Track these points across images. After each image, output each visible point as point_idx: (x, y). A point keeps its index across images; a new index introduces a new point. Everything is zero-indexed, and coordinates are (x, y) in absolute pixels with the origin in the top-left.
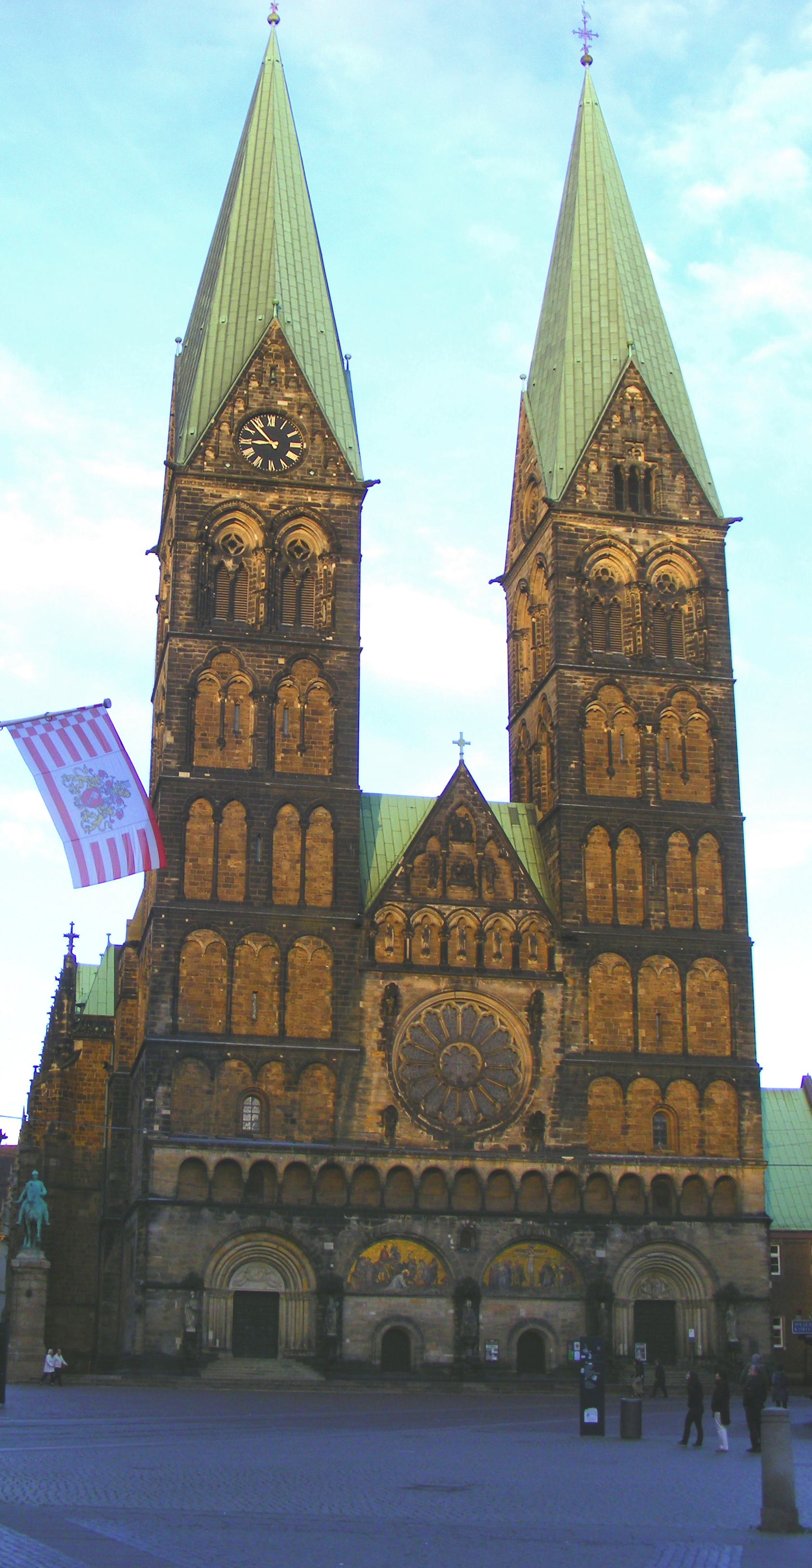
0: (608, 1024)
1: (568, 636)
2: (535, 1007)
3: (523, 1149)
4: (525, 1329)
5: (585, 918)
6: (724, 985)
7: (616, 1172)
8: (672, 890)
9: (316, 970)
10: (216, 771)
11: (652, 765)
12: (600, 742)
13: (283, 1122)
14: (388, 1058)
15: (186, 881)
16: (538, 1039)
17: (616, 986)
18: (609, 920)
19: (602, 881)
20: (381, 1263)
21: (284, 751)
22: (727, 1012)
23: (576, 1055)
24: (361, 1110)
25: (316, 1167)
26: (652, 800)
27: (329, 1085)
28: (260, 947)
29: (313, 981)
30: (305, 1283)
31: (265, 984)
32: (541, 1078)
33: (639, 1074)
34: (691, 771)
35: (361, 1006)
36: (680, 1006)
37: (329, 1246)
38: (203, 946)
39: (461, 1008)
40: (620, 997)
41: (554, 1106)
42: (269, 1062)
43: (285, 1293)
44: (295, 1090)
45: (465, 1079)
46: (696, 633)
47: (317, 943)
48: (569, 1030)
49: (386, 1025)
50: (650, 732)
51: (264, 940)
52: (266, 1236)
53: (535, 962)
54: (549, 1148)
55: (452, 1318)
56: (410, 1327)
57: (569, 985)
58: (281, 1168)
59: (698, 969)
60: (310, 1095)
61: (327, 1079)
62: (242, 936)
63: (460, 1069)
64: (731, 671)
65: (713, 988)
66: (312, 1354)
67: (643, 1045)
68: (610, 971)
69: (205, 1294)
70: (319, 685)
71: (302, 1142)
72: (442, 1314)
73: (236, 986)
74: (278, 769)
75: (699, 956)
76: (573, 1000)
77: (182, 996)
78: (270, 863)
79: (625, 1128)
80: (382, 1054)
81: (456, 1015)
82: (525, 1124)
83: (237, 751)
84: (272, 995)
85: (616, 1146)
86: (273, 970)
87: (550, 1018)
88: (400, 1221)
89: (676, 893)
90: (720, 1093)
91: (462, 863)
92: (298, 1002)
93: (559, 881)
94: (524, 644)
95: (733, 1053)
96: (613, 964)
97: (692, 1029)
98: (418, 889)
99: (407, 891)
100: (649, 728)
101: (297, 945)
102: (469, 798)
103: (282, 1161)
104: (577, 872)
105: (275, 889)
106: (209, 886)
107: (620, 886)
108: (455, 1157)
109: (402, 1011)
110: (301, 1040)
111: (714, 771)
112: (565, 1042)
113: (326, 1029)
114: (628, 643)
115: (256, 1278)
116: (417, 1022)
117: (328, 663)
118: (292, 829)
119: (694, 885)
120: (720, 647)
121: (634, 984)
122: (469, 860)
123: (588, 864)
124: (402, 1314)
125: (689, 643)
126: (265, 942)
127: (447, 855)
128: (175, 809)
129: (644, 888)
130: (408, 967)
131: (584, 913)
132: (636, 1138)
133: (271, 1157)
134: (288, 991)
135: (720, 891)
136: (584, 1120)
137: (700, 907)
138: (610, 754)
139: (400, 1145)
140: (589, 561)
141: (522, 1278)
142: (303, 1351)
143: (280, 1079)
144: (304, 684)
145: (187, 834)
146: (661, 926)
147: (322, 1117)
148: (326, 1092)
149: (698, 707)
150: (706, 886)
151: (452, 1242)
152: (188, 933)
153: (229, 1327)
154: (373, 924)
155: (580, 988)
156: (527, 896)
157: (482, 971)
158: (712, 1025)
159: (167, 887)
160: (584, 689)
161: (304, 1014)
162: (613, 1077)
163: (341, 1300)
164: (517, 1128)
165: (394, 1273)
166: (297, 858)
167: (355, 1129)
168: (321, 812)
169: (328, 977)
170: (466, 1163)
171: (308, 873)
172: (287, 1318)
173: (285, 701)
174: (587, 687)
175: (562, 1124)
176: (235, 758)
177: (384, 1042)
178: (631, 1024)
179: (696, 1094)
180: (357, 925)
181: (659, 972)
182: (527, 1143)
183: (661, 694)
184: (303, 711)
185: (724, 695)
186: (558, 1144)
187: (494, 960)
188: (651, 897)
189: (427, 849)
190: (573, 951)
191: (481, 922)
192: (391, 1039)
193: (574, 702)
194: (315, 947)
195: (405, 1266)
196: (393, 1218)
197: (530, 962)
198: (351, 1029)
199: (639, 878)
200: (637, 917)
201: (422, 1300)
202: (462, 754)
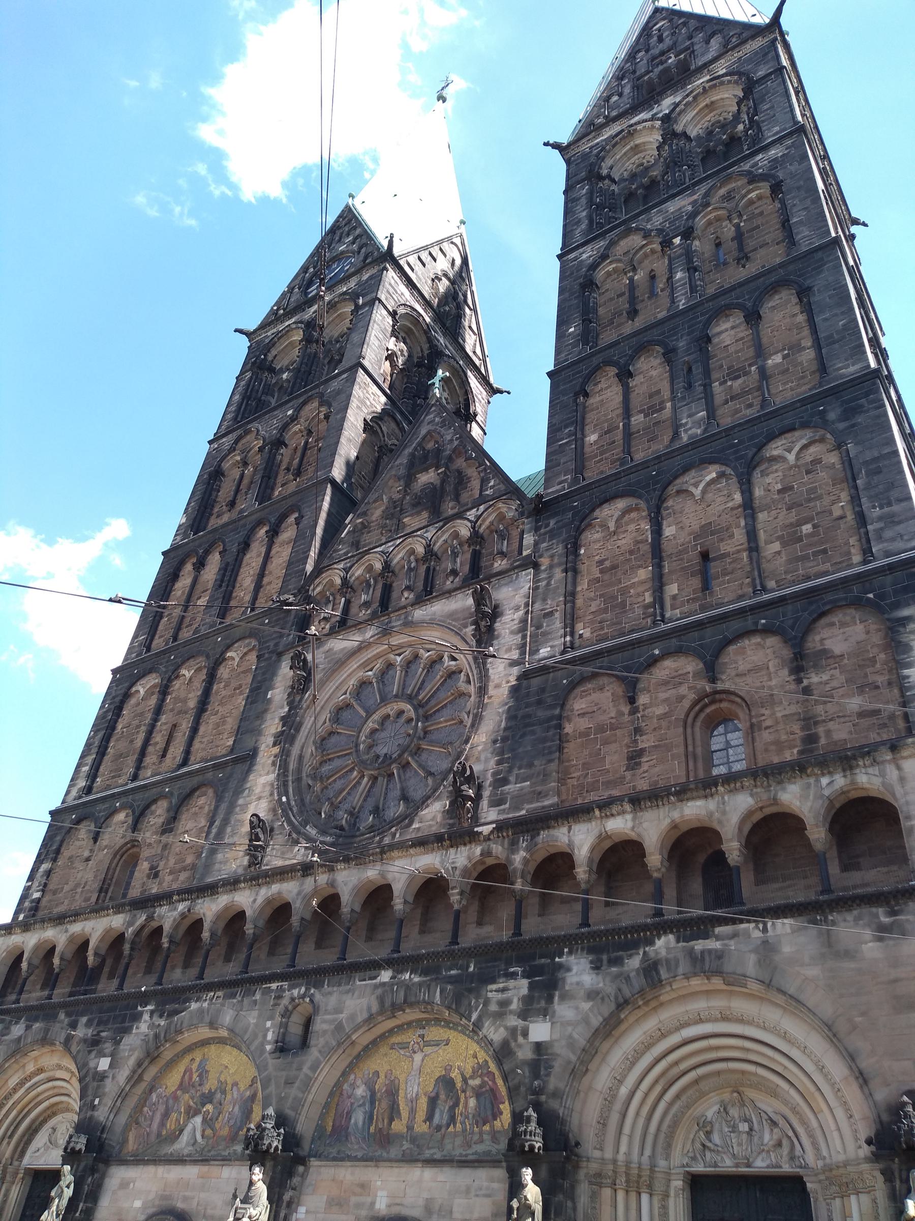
13: (145, 879)
17: (625, 541)
20: (179, 1093)
33: (657, 652)
37: (104, 1064)
38: (142, 691)
49: (290, 710)
57: (543, 568)
62: (178, 667)
67: (673, 608)
76: (548, 584)
79: (634, 758)
88: (205, 1005)
89: (729, 383)
104: (567, 431)
132: (657, 769)
140: (609, 162)
141: (393, 1112)
158: (814, 526)
165: (191, 1113)
177: (282, 733)
179: (787, 653)
181: (697, 492)
186: (501, 817)
190: (552, 522)
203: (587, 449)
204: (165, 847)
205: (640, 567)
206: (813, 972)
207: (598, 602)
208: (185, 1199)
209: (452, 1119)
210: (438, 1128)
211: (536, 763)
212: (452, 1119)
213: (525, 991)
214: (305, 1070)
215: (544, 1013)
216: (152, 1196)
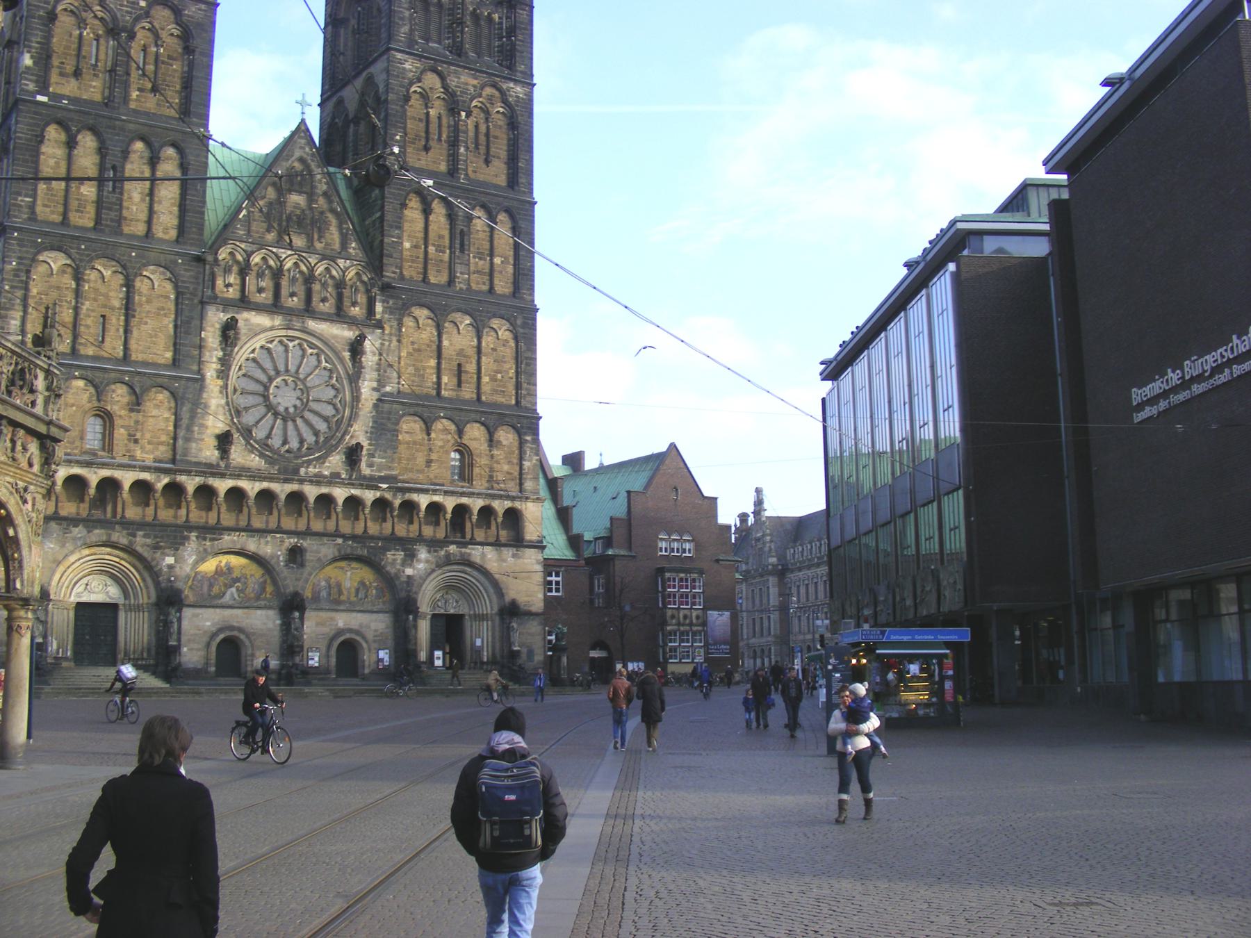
0: (416, 369)
1: (401, 23)
2: (356, 348)
3: (343, 476)
4: (342, 638)
5: (401, 273)
6: (512, 344)
7: (423, 501)
8: (474, 257)
9: (161, 299)
10: (74, 100)
11: (464, 146)
12: (420, 120)
13: (126, 442)
14: (226, 386)
15: (39, 202)
16: (359, 378)
18: (420, 277)
19: (417, 242)
21: (140, 90)
22: (514, 366)
23: (390, 394)
24: (198, 434)
25: (159, 484)
26: (462, 176)
27: (170, 409)
28: (109, 272)
29: (158, 309)
30: (145, 595)
31: (112, 308)
32: (360, 413)
33: (442, 415)
34: (494, 157)
35: (203, 336)
36: (476, 358)
39: (291, 345)
40: (428, 346)
41: (370, 439)
42: (114, 383)
43: (124, 605)
44: (139, 411)
45: (291, 410)
46: (504, 39)
47: (163, 274)
48: (385, 372)
49: (225, 355)
50: (463, 117)
51: (113, 266)
52: (108, 550)
53: (357, 309)
54: (364, 477)
55: (278, 628)
56: (242, 637)
57: (386, 332)
58: (126, 486)
59: (492, 328)
60: (152, 416)
61: (169, 402)
62: (91, 260)
63: (286, 399)
64: (532, 76)
65: (504, 345)
66: (152, 662)
68: (420, 322)
69: (51, 603)
70: (176, 32)
71: (144, 461)
72: (270, 625)
73: (84, 308)
74: (133, 105)
75: (495, 316)
76: (389, 345)
77: (31, 314)
78: (121, 193)
79: (429, 462)
80: (220, 382)
81: (287, 350)
82: (345, 453)
83: (94, 84)
84: (119, 319)
85: (421, 476)
86: (121, 295)
87: (370, 359)
88: (235, 538)
89: (477, 260)
90: (506, 437)
91: (298, 212)
92: (143, 327)
93: (380, 238)
94: (342, 31)
95: (518, 403)
96: (423, 317)
97: (485, 379)
98: (257, 232)
99: (249, 231)
100: (463, 114)
101: (145, 273)
102: (308, 154)
103: (127, 478)
105: (125, 219)
106: (61, 209)
107: (431, 249)
108: (286, 481)
109: (240, 343)
110: (146, 364)
111: (513, 159)
112: (381, 382)
113: (169, 355)
114: (448, 38)
115: (97, 590)
116: (252, 355)
117: (186, 12)
118: (144, 164)
119: (492, 255)
120: (525, 54)
121: (440, 336)
122: (303, 211)
123: (406, 226)
124: (235, 624)
125: (498, 47)
126: (114, 269)
127: (285, 202)
128: (33, 130)
129: (451, 253)
130: (244, 302)
131: (401, 268)
132: (437, 471)
133: (117, 474)
134: (134, 316)
135: (512, 262)
136: (395, 453)
137: (496, 274)
138: (427, 132)
139: (234, 467)
141: (340, 593)
142: (143, 659)
143: (126, 400)
144: (163, 29)
145: (42, 157)
146: (464, 287)
147: (164, 438)
148: (167, 415)
149: (503, 102)
150: (502, 257)
151: (281, 559)
152: (39, 252)
153: (71, 637)
154: (216, 260)
155: (396, 336)
156: (354, 249)
157: (308, 310)
158: (502, 377)
159: (21, 206)
160: (412, 71)
161: (149, 339)
162: (420, 417)
163: (180, 611)
164: (338, 457)
166: (147, 191)
167: (193, 451)
168: (171, 151)
169: (172, 306)
170: (294, 487)
171: (156, 207)
172: (126, 628)
173: (142, 42)
174: (414, 70)
175: (377, 455)
176: (92, 90)
177: (223, 370)
178: (435, 371)
179: (487, 436)
180: (199, 260)
182: (347, 470)
183: (474, 86)
184: (157, 55)
185: (525, 95)
187: (322, 304)
188: (457, 261)
189: (267, 197)
191: (313, 268)
192: (229, 369)
193: (402, 82)
194: (162, 277)
195: (237, 580)
196: (229, 535)
197: (352, 309)
198: (192, 357)
199: (447, 242)
200: (443, 278)
201: (252, 611)
202: (303, 113)
203: (405, 253)
204: (137, 422)
205: (431, 357)
206: (495, 564)
207: (411, 368)
208: (238, 622)
209: (366, 597)
210: (361, 599)
211: (388, 451)
212: (366, 597)
213: (402, 557)
214: (305, 575)
215: (411, 566)
216: (216, 620)
